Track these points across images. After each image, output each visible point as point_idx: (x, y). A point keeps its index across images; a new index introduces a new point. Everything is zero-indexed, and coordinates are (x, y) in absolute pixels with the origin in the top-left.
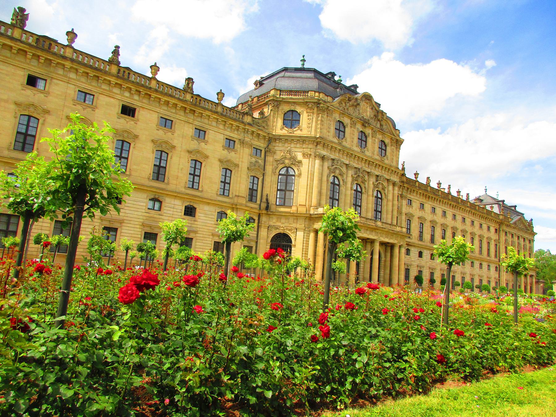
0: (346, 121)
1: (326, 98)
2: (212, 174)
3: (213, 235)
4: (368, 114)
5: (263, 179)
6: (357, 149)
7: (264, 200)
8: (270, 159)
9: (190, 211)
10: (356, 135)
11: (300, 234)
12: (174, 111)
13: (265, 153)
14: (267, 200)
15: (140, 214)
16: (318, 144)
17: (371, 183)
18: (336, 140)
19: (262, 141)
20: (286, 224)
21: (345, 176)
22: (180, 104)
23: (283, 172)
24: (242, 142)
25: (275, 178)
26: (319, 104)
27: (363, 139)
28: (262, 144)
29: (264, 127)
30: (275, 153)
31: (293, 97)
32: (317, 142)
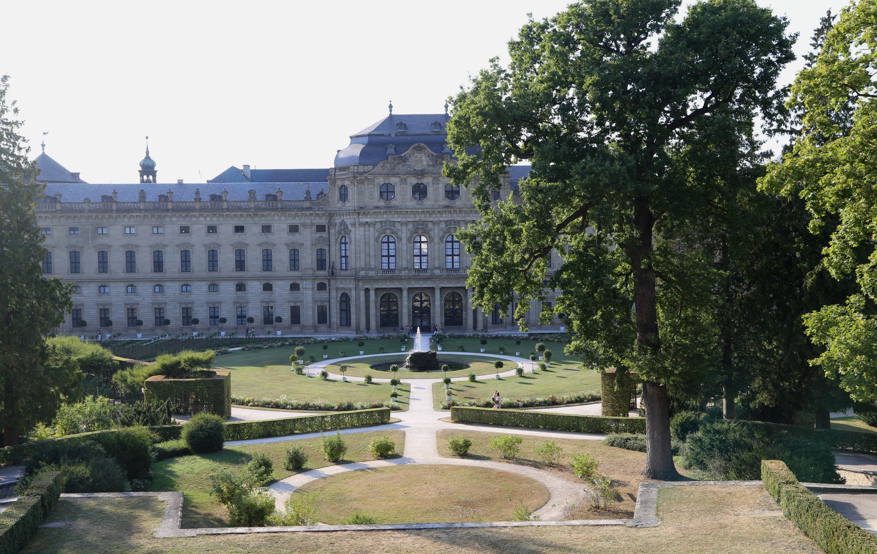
0: (394, 180)
1: (366, 168)
3: (289, 302)
4: (425, 163)
6: (411, 203)
8: (332, 231)
9: (268, 287)
10: (410, 189)
11: (353, 292)
12: (242, 219)
16: (359, 214)
17: (436, 231)
18: (382, 203)
19: (324, 218)
21: (399, 233)
22: (245, 214)
24: (304, 225)
25: (338, 245)
27: (420, 191)
28: (323, 221)
32: (361, 211)
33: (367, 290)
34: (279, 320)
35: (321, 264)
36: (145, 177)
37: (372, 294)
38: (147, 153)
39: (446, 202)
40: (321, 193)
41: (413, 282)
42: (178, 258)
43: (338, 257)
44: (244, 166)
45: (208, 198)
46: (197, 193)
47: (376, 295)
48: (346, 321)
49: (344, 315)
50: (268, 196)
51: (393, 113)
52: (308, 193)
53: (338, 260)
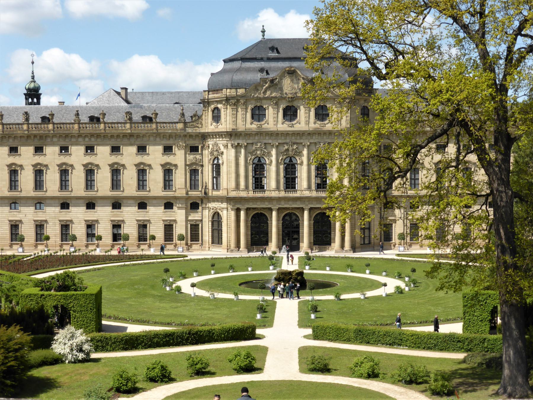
2: (155, 178)
5: (202, 170)
7: (204, 187)
8: (206, 152)
11: (225, 212)
12: (119, 140)
13: (202, 147)
14: (206, 186)
15: (107, 213)
20: (218, 205)
23: (216, 162)
25: (210, 167)
26: (230, 100)
29: (198, 127)
30: (209, 147)
31: (216, 95)
32: (232, 135)
33: (238, 211)
34: (153, 238)
35: (194, 184)
36: (30, 100)
37: (242, 213)
38: (33, 77)
39: (318, 125)
40: (195, 115)
41: (283, 203)
42: (57, 176)
43: (210, 177)
44: (122, 88)
45: (87, 120)
46: (77, 115)
47: (247, 214)
48: (217, 239)
49: (216, 234)
50: (144, 118)
51: (266, 37)
52: (183, 115)
53: (210, 180)
